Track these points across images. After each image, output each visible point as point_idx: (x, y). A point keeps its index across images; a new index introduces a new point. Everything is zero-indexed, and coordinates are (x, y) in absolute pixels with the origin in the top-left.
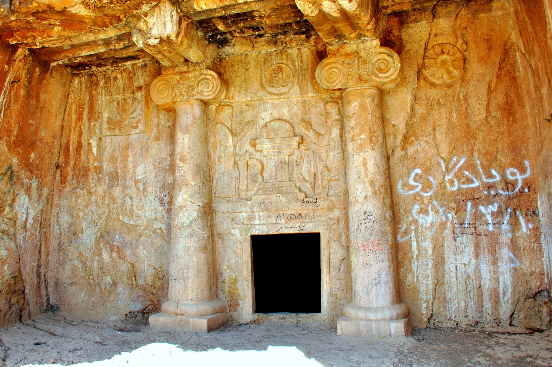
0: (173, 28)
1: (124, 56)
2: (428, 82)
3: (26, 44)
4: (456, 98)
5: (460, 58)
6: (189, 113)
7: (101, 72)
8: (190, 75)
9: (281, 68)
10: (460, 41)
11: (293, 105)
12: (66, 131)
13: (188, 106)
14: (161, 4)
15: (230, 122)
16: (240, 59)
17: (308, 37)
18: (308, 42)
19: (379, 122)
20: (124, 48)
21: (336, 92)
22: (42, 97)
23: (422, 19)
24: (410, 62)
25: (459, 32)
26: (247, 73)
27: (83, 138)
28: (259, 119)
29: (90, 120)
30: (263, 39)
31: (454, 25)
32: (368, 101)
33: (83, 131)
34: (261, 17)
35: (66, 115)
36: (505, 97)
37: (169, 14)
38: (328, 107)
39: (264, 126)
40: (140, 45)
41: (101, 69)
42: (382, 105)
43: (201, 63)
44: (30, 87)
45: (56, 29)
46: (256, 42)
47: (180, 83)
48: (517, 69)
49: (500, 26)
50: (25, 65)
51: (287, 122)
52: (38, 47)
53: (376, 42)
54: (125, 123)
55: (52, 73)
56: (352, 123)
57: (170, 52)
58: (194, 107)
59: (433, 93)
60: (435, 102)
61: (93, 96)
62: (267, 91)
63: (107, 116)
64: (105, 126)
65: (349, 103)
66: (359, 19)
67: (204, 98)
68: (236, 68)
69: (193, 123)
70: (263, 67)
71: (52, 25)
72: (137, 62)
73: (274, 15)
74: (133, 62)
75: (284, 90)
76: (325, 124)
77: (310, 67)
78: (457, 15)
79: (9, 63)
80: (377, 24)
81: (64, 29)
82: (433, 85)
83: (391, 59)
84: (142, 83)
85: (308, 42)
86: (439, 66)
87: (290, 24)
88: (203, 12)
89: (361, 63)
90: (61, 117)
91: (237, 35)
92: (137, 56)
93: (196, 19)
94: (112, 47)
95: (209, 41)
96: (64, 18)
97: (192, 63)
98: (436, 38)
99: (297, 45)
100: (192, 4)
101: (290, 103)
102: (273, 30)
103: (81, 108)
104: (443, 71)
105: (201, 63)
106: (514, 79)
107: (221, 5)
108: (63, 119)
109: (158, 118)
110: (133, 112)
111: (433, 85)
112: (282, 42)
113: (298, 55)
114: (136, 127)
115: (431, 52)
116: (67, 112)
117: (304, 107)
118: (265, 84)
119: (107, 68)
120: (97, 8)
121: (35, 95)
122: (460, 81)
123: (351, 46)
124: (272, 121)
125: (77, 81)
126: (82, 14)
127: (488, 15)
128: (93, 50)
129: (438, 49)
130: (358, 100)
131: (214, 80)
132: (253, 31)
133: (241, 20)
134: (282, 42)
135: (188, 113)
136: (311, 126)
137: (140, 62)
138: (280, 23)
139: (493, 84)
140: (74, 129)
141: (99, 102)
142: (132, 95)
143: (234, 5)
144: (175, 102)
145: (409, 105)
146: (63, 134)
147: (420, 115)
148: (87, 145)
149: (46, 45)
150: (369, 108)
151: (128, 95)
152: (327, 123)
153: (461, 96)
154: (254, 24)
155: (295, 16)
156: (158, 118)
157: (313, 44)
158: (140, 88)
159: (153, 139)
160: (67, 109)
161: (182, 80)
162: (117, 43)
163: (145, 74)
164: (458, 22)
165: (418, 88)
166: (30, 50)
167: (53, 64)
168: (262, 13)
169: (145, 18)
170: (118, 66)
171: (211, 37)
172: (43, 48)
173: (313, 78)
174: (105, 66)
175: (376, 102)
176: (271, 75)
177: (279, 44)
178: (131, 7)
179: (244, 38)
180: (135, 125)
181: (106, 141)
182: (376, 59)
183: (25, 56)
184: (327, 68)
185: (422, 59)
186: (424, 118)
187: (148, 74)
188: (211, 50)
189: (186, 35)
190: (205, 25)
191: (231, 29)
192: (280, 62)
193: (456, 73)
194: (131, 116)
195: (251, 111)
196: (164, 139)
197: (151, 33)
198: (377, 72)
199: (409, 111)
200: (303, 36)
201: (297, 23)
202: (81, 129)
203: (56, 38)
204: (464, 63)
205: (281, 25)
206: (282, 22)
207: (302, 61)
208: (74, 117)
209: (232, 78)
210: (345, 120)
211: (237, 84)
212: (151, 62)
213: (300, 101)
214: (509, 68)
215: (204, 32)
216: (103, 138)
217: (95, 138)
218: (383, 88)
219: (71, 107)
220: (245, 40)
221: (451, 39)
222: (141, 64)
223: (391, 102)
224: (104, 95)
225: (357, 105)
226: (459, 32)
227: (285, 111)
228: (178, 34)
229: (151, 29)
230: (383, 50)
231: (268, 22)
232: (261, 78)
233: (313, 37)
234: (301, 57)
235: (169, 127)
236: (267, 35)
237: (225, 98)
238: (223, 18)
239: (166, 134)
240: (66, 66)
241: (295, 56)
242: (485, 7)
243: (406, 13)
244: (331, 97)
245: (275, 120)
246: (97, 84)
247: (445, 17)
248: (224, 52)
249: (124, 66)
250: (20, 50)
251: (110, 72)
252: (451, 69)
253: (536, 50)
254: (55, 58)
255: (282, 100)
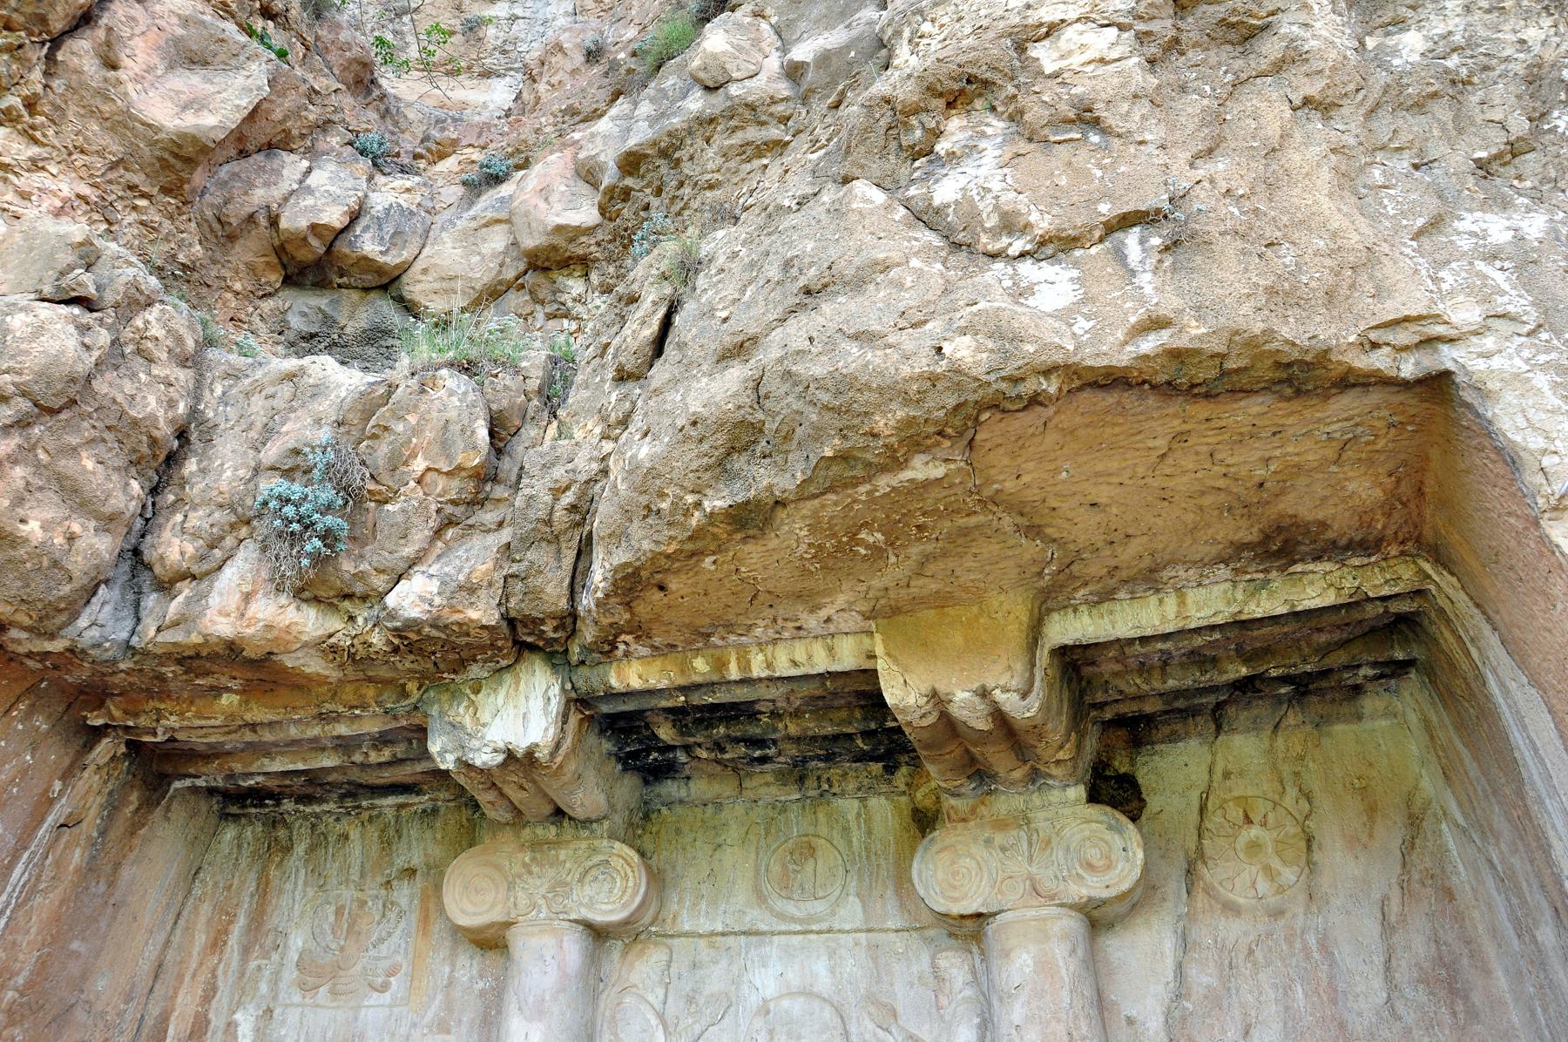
0: (546, 729)
1: (381, 781)
2: (1217, 900)
3: (127, 728)
4: (1298, 945)
5: (1295, 835)
6: (546, 959)
7: (305, 818)
8: (562, 854)
9: (812, 850)
10: (1292, 792)
11: (843, 952)
12: (168, 976)
13: (548, 941)
14: (522, 668)
15: (660, 992)
16: (699, 816)
17: (891, 769)
18: (890, 782)
19: (1094, 1012)
20: (389, 764)
21: (968, 923)
22: (126, 873)
23: (1187, 735)
24: (1163, 844)
25: (1286, 769)
26: (717, 855)
27: (214, 1002)
28: (745, 989)
29: (246, 951)
30: (768, 767)
31: (1271, 750)
32: (1060, 951)
33: (220, 983)
34: (775, 715)
35: (178, 932)
36: (1433, 946)
37: (540, 691)
38: (942, 963)
39: (758, 1013)
40: (448, 763)
41: (308, 810)
42: (1094, 962)
43: (597, 821)
44: (103, 844)
45: (226, 699)
46: (749, 775)
47: (530, 873)
48: (1449, 869)
49: (1388, 755)
50: (105, 782)
51: (824, 1000)
52: (158, 739)
53: (1078, 792)
54: (351, 971)
55: (168, 809)
56: (1017, 1013)
57: (522, 787)
58: (565, 944)
59: (1234, 930)
60: (1242, 957)
61: (267, 884)
62: (771, 910)
63: (300, 944)
64: (290, 974)
65: (1006, 954)
66: (1041, 737)
67: (598, 918)
68: (688, 839)
69: (558, 992)
70: (762, 842)
71: (217, 691)
72: (413, 799)
73: (811, 712)
74: (401, 799)
75: (819, 907)
76: (934, 1010)
77: (892, 848)
78: (1276, 727)
79: (67, 775)
80: (1079, 747)
81: (247, 702)
82: (1231, 909)
83: (1117, 837)
84: (417, 860)
85: (890, 782)
86: (1242, 856)
87: (849, 737)
88: (629, 694)
89: (1036, 847)
90: (161, 937)
91: (704, 755)
92: (415, 785)
93: (605, 708)
94: (358, 758)
95: (625, 764)
96: (257, 675)
97: (570, 818)
98: (1228, 783)
99: (859, 789)
100: (606, 674)
101: (833, 945)
102: (803, 747)
103: (227, 914)
104: (1254, 869)
105: (597, 821)
106: (1449, 894)
107: (681, 681)
108: (168, 942)
109: (453, 966)
110: (381, 940)
111: (1231, 909)
112: (819, 778)
113: (859, 815)
114: (384, 988)
115: (1218, 819)
116: (181, 922)
117: (875, 959)
118: (767, 888)
119: (325, 807)
120: (354, 660)
121: (108, 869)
122: (1302, 897)
123: (1006, 803)
124: (782, 996)
125: (230, 833)
126: (308, 670)
127: (1354, 727)
128: (305, 760)
129: (1236, 813)
130: (1032, 948)
131: (629, 870)
132: (747, 747)
133: (721, 719)
134: (819, 778)
135: (548, 958)
136: (895, 1016)
137: (421, 802)
138: (823, 732)
139: (1394, 906)
140: (194, 975)
141: (285, 901)
142: (383, 892)
143: (713, 684)
144: (508, 925)
145: (1170, 963)
146: (157, 986)
147: (1202, 991)
148: (222, 1026)
149: (180, 736)
150: (1063, 972)
151: (373, 888)
152: (939, 1008)
153: (1312, 940)
154: (754, 730)
155: (865, 719)
156: (453, 966)
157: (903, 787)
158: (411, 872)
159: (430, 1027)
160: (185, 913)
161: (541, 865)
162: (375, 747)
163: (429, 834)
164: (1280, 741)
165: (1191, 917)
166: (129, 744)
167: (177, 784)
168: (779, 704)
169: (472, 697)
170: (358, 807)
171: (634, 755)
172: (172, 740)
173: (902, 881)
174: (321, 801)
175: (1080, 953)
176: (784, 866)
177: (811, 783)
178: (442, 666)
179: (718, 762)
180: (380, 980)
181: (283, 1022)
182: (1078, 837)
183: (113, 758)
184: (946, 856)
185: (1195, 837)
186: (1215, 1001)
187: (439, 836)
188: (628, 788)
189: (573, 750)
190: (622, 724)
191: (692, 740)
192: (811, 830)
193: (1289, 875)
194: (372, 953)
195: (724, 963)
196: (464, 1029)
197: (483, 737)
198: (1080, 871)
199: (1171, 978)
200: (876, 768)
201: (867, 734)
202: (214, 976)
203: (218, 723)
204: (1309, 848)
205: (825, 738)
206: (830, 730)
207: (869, 833)
208: (201, 939)
209: (674, 867)
210: (995, 1003)
211: (688, 883)
212: (452, 804)
213: (864, 943)
214: (1428, 865)
215: (618, 742)
216: (277, 1012)
217: (251, 1008)
218: (1096, 913)
219: (196, 908)
220: (719, 768)
221: (1268, 787)
222: (421, 807)
223: (1120, 954)
224: (300, 882)
225: (1029, 962)
226: (1286, 769)
227: (821, 967)
228: (558, 746)
229: (484, 725)
230: (1095, 811)
231: (793, 729)
232: (757, 871)
233: (904, 770)
234: (868, 821)
235: (482, 993)
236: (782, 759)
237: (651, 924)
238: (676, 714)
239: (469, 1014)
240: (211, 791)
241: (851, 817)
242: (1346, 709)
243: (1149, 719)
244: (950, 935)
245: (790, 994)
246: (288, 849)
247: (1248, 730)
248: (659, 795)
249: (373, 807)
250: (105, 741)
251: (331, 820)
252: (1276, 863)
253: (1500, 823)
254: (192, 771)
255: (813, 937)
